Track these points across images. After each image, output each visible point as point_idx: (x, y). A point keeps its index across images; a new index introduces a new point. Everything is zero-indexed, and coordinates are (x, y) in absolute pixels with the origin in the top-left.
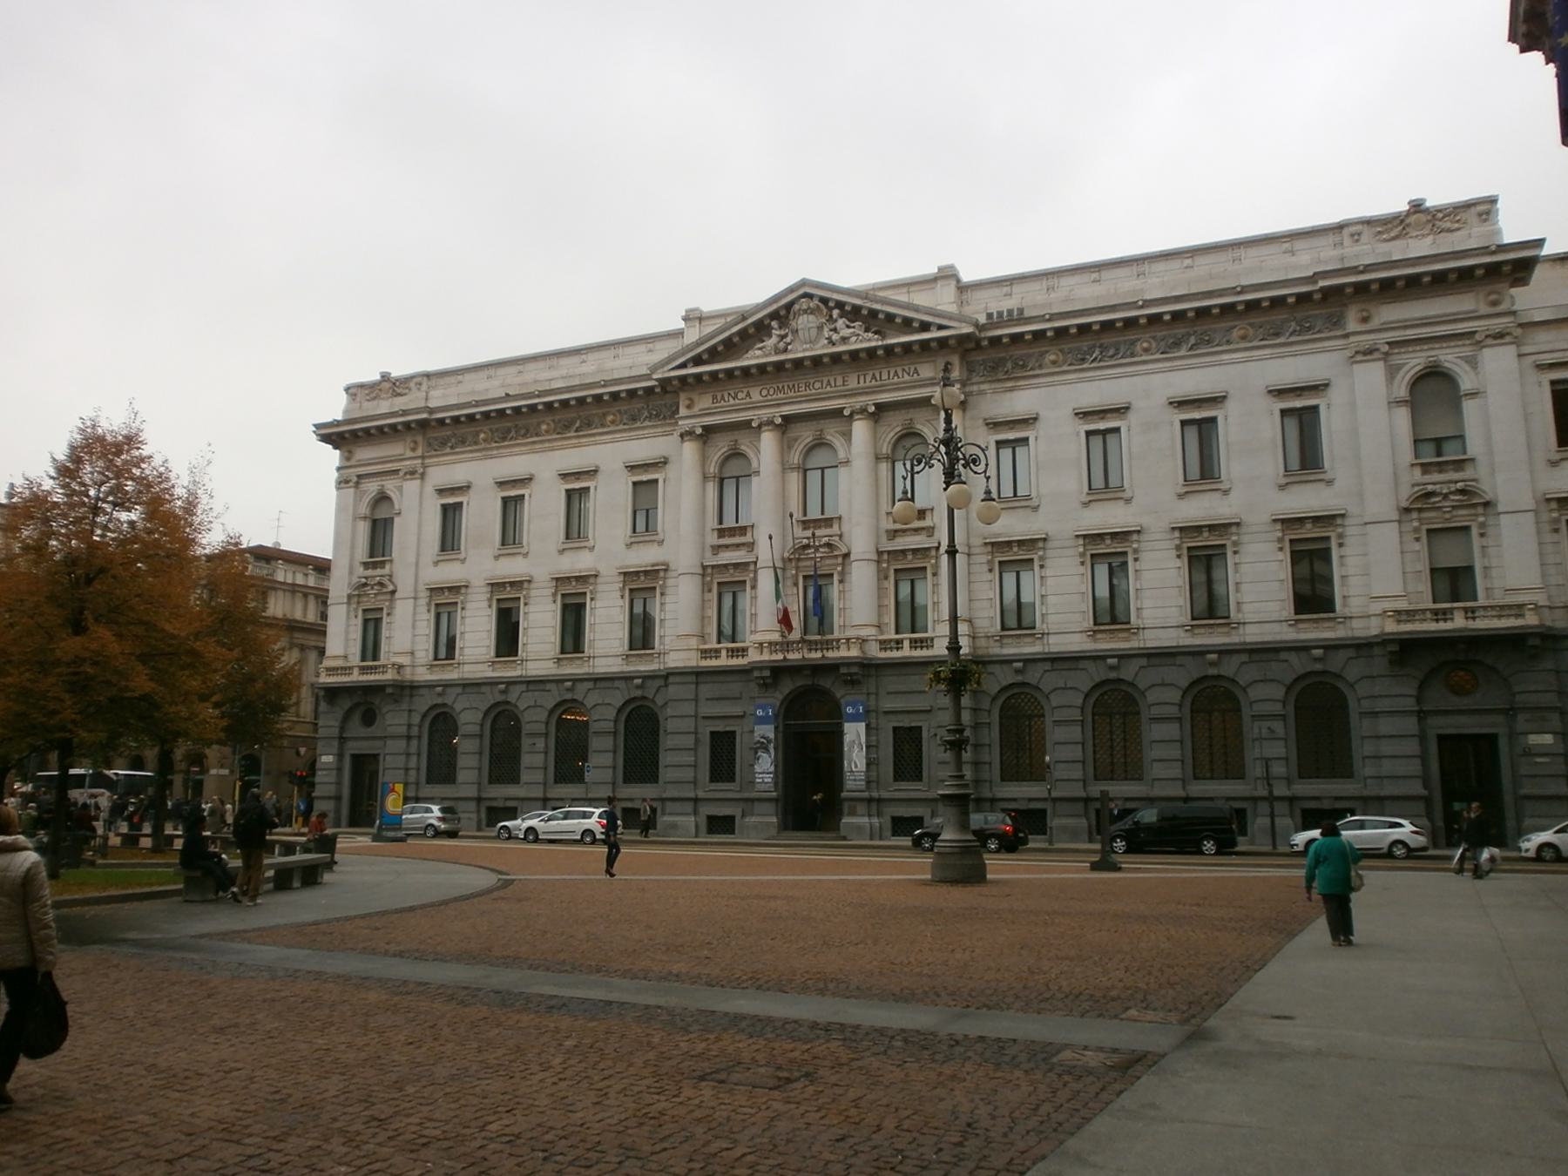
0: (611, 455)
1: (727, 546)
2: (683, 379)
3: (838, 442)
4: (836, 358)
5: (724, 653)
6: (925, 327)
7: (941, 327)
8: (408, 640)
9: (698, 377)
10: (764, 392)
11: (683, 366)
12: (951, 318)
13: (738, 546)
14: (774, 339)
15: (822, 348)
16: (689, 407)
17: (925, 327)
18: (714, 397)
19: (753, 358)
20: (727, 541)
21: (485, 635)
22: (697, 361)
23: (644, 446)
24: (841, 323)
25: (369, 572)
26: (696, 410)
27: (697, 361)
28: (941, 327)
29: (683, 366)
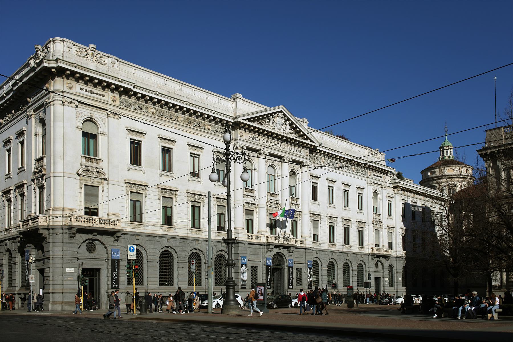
1: (248, 196)
2: (245, 124)
3: (277, 166)
5: (254, 237)
6: (308, 138)
7: (311, 141)
8: (114, 208)
11: (245, 120)
13: (251, 196)
16: (241, 136)
17: (308, 138)
24: (288, 126)
25: (89, 163)
26: (243, 138)
27: (249, 119)
28: (311, 141)
29: (245, 120)
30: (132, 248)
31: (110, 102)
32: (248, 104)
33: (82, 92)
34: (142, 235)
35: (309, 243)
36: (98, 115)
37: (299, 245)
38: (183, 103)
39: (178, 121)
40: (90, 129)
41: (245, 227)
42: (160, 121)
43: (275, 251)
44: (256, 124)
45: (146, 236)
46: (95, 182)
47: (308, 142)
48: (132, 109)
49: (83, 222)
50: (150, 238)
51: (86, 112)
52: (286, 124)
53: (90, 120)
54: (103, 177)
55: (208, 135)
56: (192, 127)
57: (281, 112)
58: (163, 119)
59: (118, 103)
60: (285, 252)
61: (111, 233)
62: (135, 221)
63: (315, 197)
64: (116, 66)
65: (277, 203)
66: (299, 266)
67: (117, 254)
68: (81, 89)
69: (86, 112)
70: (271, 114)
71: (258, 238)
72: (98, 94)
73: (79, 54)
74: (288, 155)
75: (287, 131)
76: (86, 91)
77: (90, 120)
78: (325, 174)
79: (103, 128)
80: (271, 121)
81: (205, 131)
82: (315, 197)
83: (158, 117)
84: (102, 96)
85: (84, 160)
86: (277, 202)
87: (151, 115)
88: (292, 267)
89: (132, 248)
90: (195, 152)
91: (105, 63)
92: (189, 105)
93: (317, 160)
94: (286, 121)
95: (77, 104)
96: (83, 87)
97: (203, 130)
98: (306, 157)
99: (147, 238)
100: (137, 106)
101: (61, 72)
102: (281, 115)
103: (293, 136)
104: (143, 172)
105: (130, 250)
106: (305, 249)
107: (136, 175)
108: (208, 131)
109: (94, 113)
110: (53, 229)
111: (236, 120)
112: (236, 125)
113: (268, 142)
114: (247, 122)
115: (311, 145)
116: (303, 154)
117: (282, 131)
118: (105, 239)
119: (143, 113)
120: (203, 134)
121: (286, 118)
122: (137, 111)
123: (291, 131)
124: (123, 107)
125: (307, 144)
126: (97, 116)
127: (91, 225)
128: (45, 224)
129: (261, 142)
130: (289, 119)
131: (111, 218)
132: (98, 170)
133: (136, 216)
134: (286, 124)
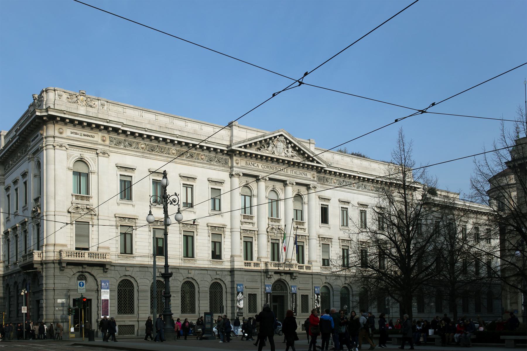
0: (204, 173)
1: (246, 222)
2: (240, 152)
4: (289, 162)
6: (313, 160)
7: (318, 162)
8: (105, 242)
9: (246, 153)
10: (263, 167)
11: (241, 147)
12: (322, 161)
13: (250, 223)
14: (270, 148)
15: (282, 157)
16: (237, 164)
17: (313, 160)
18: (246, 163)
19: (264, 152)
20: (246, 220)
21: (147, 244)
22: (245, 147)
23: (220, 174)
24: (290, 150)
25: (79, 201)
27: (245, 147)
28: (318, 162)
29: (241, 147)
30: (81, 284)
31: (100, 141)
32: (245, 130)
33: (73, 135)
34: (133, 266)
35: (317, 268)
36: (88, 156)
37: (305, 270)
38: (173, 137)
39: (169, 154)
40: (81, 168)
41: (242, 254)
42: (151, 156)
43: (276, 277)
44: (253, 151)
45: (136, 267)
46: (86, 218)
47: (315, 164)
48: (122, 147)
49: (73, 257)
50: (141, 269)
51: (76, 154)
52: (288, 148)
53: (81, 160)
54: (93, 213)
55: (201, 165)
56: (184, 158)
57: (281, 135)
58: (153, 153)
59: (107, 142)
60: (287, 278)
61: (103, 266)
62: (125, 253)
63: (325, 219)
64: (105, 107)
65: (279, 229)
66: (305, 293)
67: (106, 285)
68: (72, 133)
69: (76, 154)
70: (270, 139)
71: (256, 265)
72: (88, 136)
73: (70, 100)
74: (291, 179)
75: (289, 154)
76: (76, 134)
77: (81, 160)
78: (335, 195)
79: (93, 167)
80: (271, 146)
81: (199, 161)
82: (325, 219)
83: (149, 152)
84: (92, 137)
85: (74, 198)
86: (280, 227)
87: (141, 150)
88: (296, 294)
89: (81, 284)
90: (188, 183)
91: (95, 106)
92: (180, 138)
93: (327, 181)
94: (287, 144)
95: (68, 147)
96: (73, 131)
97: (196, 160)
98: (312, 179)
99: (138, 269)
100: (127, 143)
101: (53, 119)
102: (282, 138)
103: (297, 159)
104: (133, 206)
105: (80, 285)
106: (312, 274)
107: (126, 209)
108: (201, 161)
109: (85, 153)
110: (46, 263)
111: (229, 149)
112: (231, 153)
113: (268, 167)
114: (242, 149)
115: (317, 167)
116: (309, 177)
117: (283, 154)
118: (95, 271)
119: (134, 149)
120: (196, 164)
121: (288, 141)
122: (127, 148)
123: (293, 154)
124: (113, 145)
125: (313, 166)
126: (87, 156)
127: (83, 259)
128: (39, 259)
129: (260, 168)
130: (290, 142)
131: (101, 251)
132: (88, 207)
133: (127, 247)
134: (288, 148)
